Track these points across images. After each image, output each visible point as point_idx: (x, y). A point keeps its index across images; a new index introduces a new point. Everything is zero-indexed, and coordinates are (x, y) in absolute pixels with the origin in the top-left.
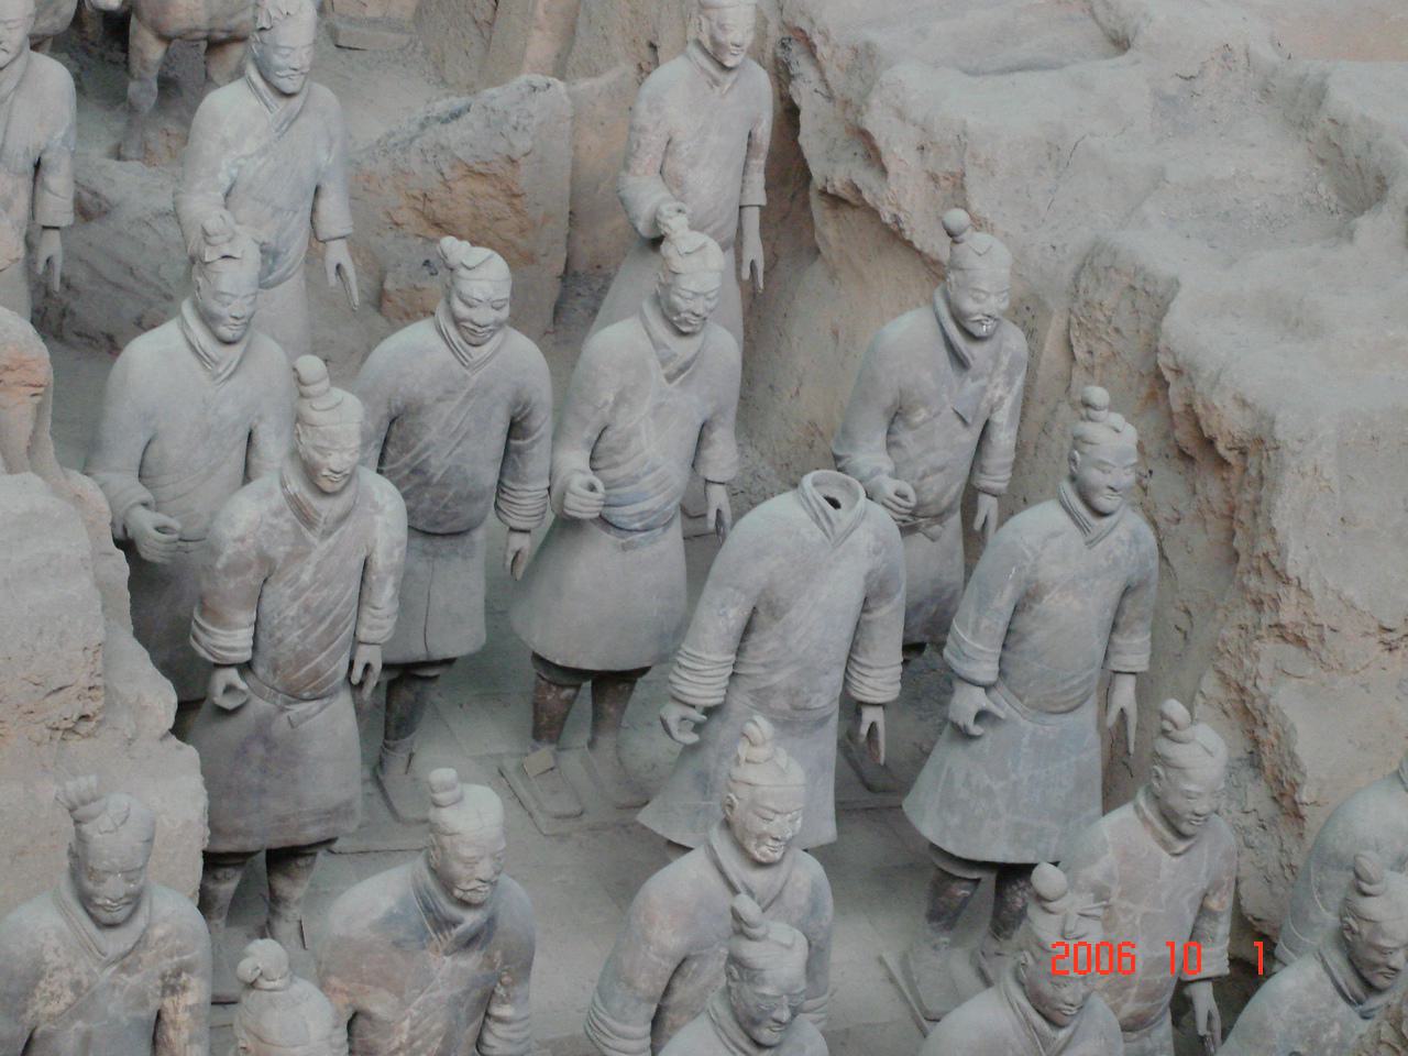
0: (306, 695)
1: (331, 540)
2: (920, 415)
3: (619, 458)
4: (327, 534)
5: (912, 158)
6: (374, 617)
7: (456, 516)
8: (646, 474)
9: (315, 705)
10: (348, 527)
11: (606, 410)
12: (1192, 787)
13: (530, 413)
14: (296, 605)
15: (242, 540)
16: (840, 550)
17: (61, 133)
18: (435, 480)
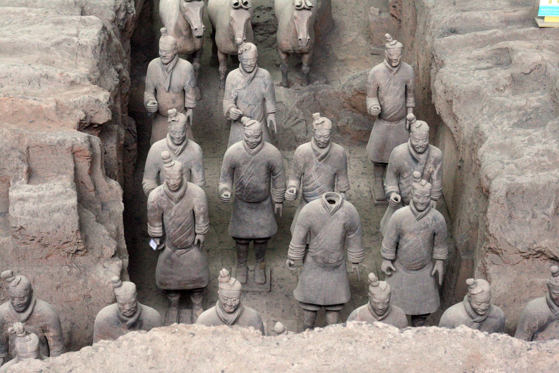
0: (179, 247)
1: (178, 204)
2: (406, 175)
3: (307, 183)
4: (177, 202)
5: (442, 94)
6: (198, 227)
7: (254, 197)
8: (316, 188)
9: (184, 251)
10: (184, 200)
11: (302, 168)
12: (376, 301)
13: (274, 168)
14: (171, 222)
15: (153, 202)
16: (333, 217)
17: (188, 82)
18: (246, 187)
